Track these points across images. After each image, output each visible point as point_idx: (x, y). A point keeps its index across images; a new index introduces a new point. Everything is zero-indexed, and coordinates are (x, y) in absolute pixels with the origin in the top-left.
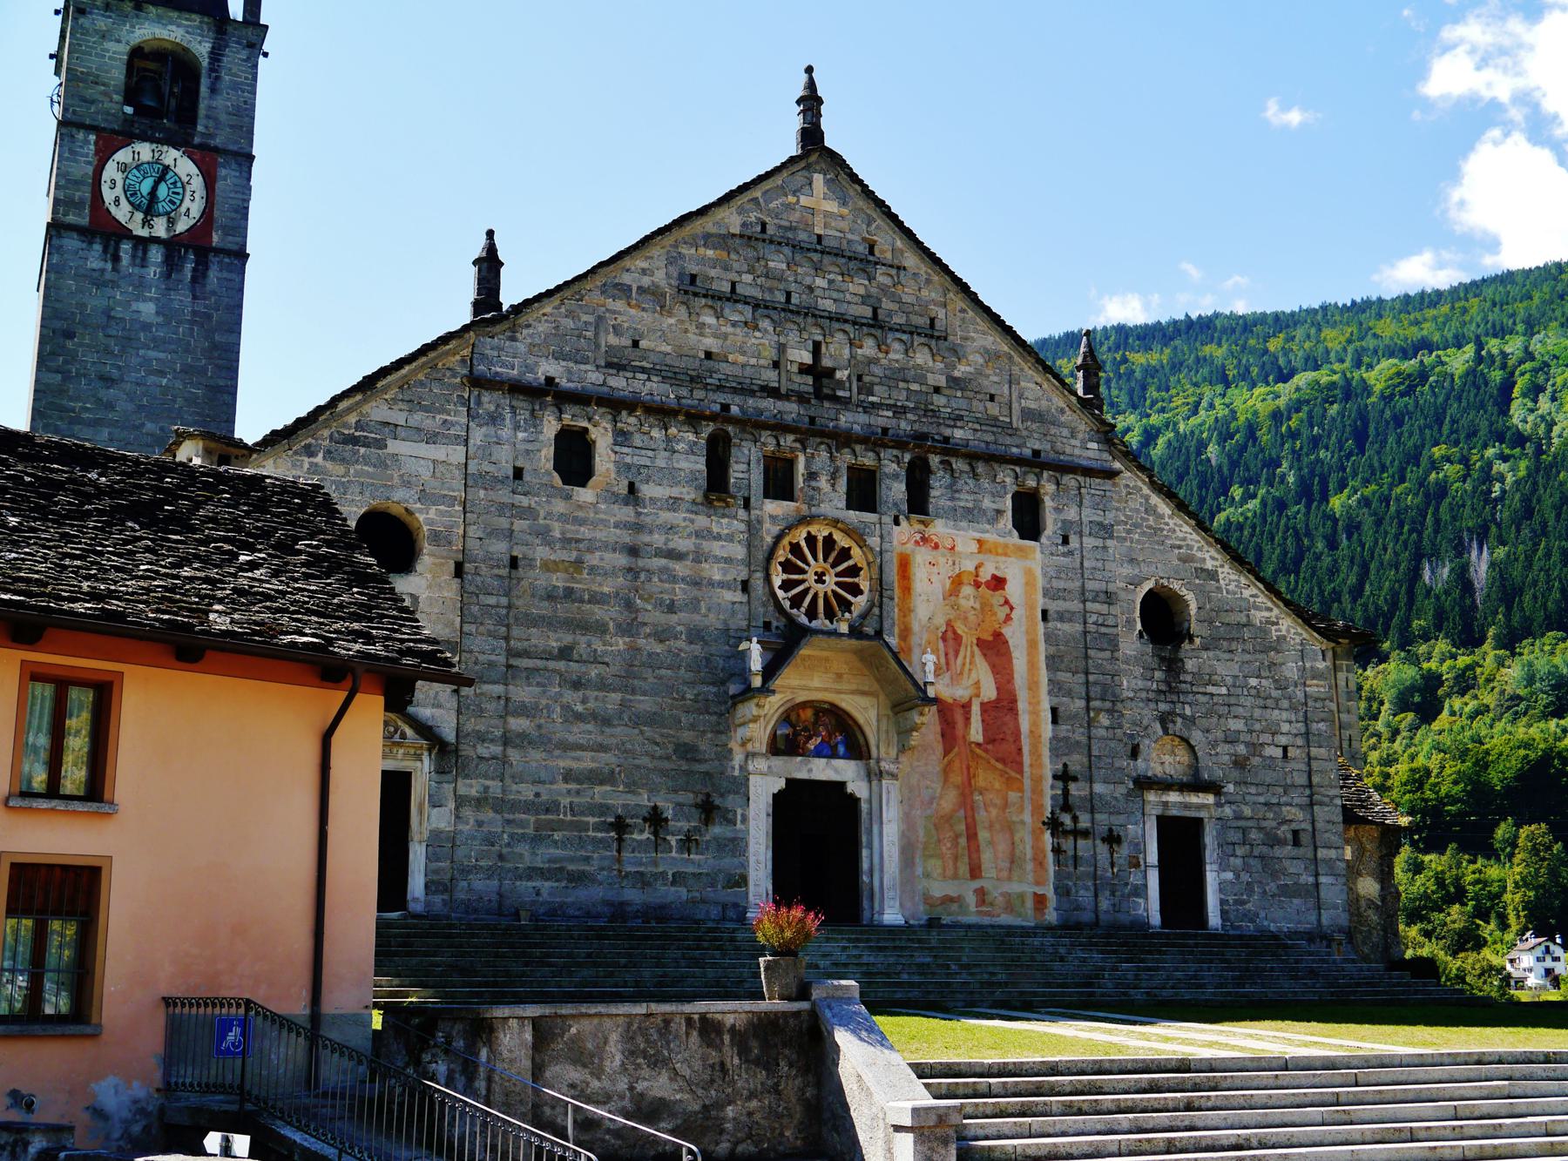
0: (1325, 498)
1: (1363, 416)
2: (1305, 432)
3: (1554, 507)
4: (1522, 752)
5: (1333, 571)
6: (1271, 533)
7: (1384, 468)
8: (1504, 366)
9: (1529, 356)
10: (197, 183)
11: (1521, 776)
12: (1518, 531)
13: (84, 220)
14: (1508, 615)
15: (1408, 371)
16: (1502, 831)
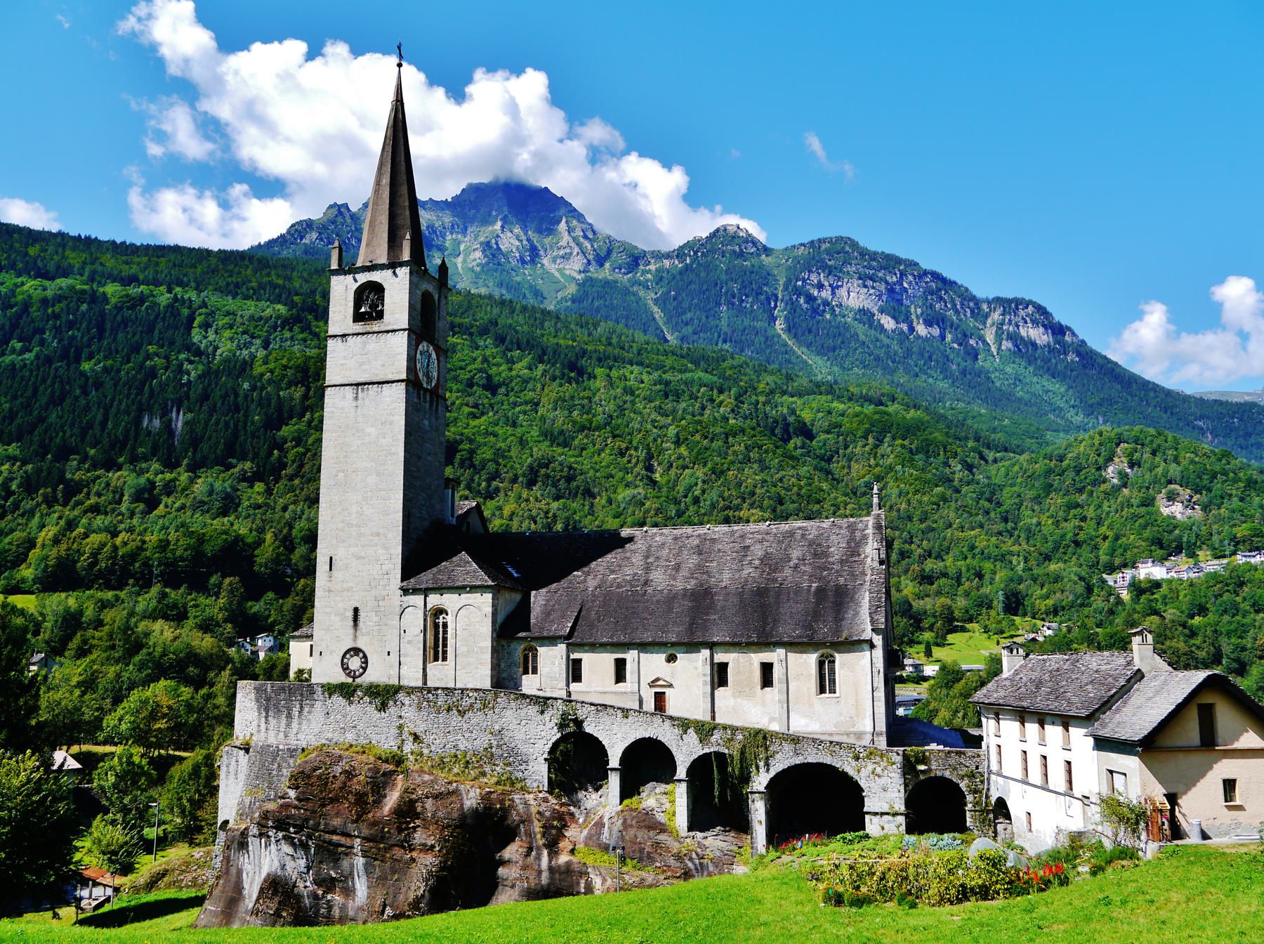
0: (78, 361)
1: (102, 315)
2: (63, 316)
3: (221, 396)
4: (224, 537)
5: (87, 409)
6: (43, 377)
7: (117, 352)
8: (190, 307)
9: (204, 305)
11: (223, 550)
12: (201, 406)
13: (412, 378)
14: (194, 453)
15: (133, 295)
16: (214, 580)
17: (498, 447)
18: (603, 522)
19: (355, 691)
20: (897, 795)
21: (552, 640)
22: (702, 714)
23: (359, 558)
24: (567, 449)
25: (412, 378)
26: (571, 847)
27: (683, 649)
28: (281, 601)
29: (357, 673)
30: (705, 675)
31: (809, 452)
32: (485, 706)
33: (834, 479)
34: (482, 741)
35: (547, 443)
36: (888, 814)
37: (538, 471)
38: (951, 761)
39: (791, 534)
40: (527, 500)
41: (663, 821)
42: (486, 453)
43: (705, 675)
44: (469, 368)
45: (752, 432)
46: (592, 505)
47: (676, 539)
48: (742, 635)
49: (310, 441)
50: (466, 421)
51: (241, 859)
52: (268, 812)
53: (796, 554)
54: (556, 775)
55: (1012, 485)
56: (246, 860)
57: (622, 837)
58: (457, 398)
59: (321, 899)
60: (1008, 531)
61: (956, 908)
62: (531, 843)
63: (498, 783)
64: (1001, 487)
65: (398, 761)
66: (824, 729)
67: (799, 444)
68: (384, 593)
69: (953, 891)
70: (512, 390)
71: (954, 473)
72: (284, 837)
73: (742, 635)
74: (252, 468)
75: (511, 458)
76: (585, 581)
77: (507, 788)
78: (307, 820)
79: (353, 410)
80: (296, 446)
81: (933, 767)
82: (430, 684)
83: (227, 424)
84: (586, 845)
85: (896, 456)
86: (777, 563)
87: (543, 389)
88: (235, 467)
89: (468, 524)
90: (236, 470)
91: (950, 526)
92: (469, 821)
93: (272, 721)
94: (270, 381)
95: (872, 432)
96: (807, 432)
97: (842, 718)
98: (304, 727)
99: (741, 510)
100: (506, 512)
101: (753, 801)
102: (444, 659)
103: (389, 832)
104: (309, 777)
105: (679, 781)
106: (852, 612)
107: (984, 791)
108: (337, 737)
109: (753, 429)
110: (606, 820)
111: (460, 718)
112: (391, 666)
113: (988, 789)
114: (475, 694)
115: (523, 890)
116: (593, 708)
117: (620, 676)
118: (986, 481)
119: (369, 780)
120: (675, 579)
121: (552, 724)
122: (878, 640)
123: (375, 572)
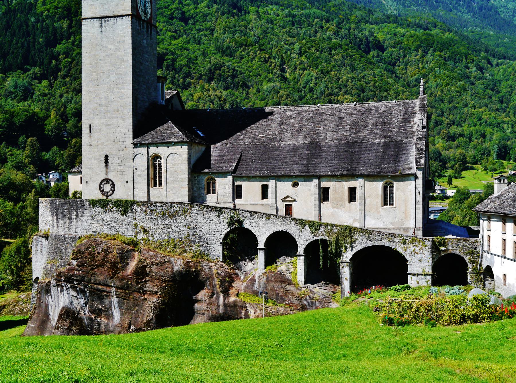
4: (26, 113)
10: (150, 3)
11: (25, 121)
12: (6, 33)
13: (135, 13)
16: (21, 139)
17: (189, 57)
18: (254, 103)
19: (108, 204)
20: (427, 264)
21: (224, 174)
22: (313, 217)
23: (107, 125)
24: (232, 58)
25: (135, 13)
26: (236, 293)
27: (302, 179)
28: (62, 152)
29: (109, 194)
30: (315, 194)
31: (381, 59)
32: (185, 213)
33: (396, 77)
34: (183, 233)
35: (220, 55)
36: (421, 275)
37: (214, 72)
38: (461, 245)
39: (369, 110)
40: (208, 90)
41: (290, 278)
42: (181, 61)
43: (315, 194)
44: (170, 7)
45: (346, 47)
46: (247, 93)
47: (298, 113)
48: (338, 171)
49: (75, 54)
50: (170, 41)
51: (47, 299)
52: (61, 273)
53: (371, 122)
54: (228, 252)
55: (507, 80)
56: (50, 299)
57: (266, 287)
58: (164, 26)
59: (93, 321)
60: (502, 109)
61: (458, 327)
62: (213, 290)
63: (193, 257)
64: (500, 81)
65: (135, 244)
66: (385, 226)
67: (375, 55)
68: (123, 146)
69: (457, 318)
70: (198, 21)
71: (471, 73)
72: (71, 287)
73: (338, 171)
74: (40, 71)
75: (198, 64)
76: (243, 138)
77: (199, 259)
78: (83, 277)
79: (99, 34)
80: (66, 57)
81: (450, 248)
82: (152, 200)
83: (23, 43)
84: (245, 291)
85: (436, 62)
86: (360, 128)
87: (217, 21)
88: (30, 70)
89: (172, 104)
90: (31, 72)
91: (467, 105)
92: (177, 278)
93: (61, 222)
94: (47, 16)
95: (421, 47)
96: (380, 47)
97: (397, 219)
98: (79, 224)
99: (339, 95)
100: (195, 97)
101: (343, 267)
102: (160, 185)
103: (131, 284)
104: (83, 253)
105: (300, 255)
106: (405, 157)
107: (479, 262)
108: (98, 230)
109: (347, 45)
110: (256, 278)
111: (170, 220)
112: (129, 190)
113: (481, 261)
114: (179, 206)
115: (209, 316)
116: (249, 214)
117: (265, 195)
118: (491, 77)
119: (119, 255)
120: (298, 137)
121: (225, 223)
122: (420, 174)
123: (117, 134)
